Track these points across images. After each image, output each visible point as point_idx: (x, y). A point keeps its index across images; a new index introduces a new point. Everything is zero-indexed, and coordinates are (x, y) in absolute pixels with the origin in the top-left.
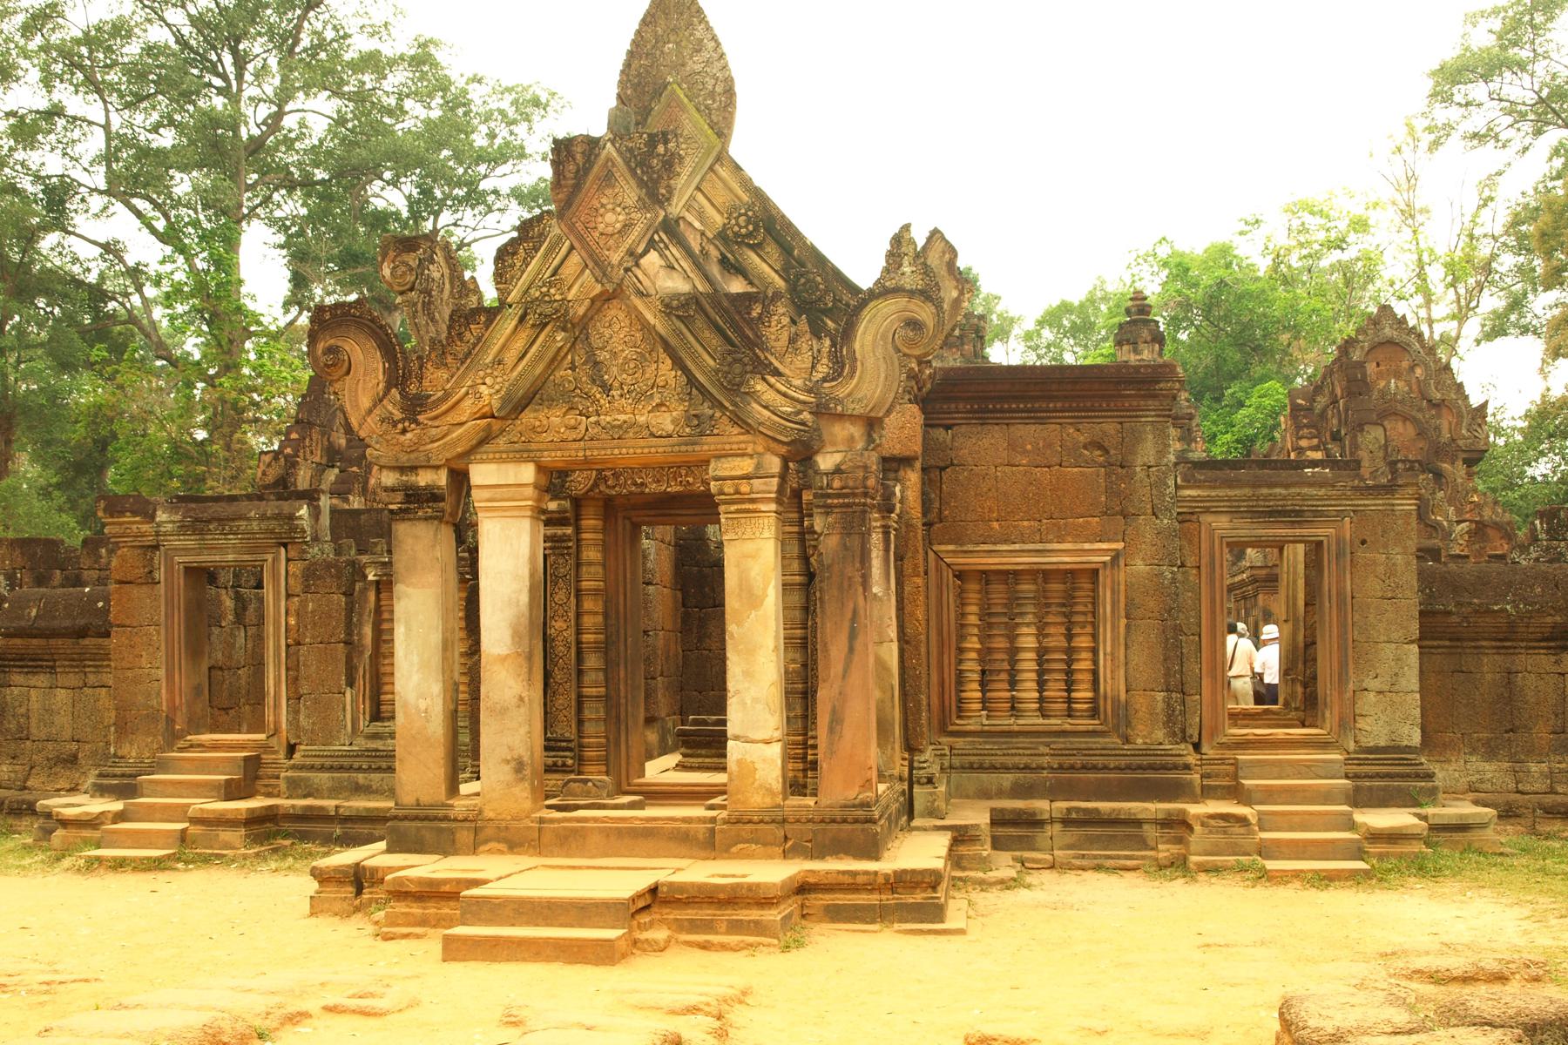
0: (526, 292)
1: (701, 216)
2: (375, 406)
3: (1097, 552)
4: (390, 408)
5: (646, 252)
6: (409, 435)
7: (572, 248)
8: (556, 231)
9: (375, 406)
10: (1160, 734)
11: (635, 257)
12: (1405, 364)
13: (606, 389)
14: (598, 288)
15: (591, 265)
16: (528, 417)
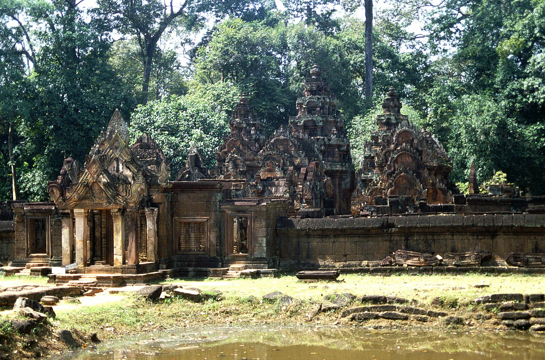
1: (122, 157)
3: (204, 219)
8: (86, 171)
10: (215, 255)
11: (98, 176)
12: (411, 138)
13: (95, 197)
16: (83, 201)
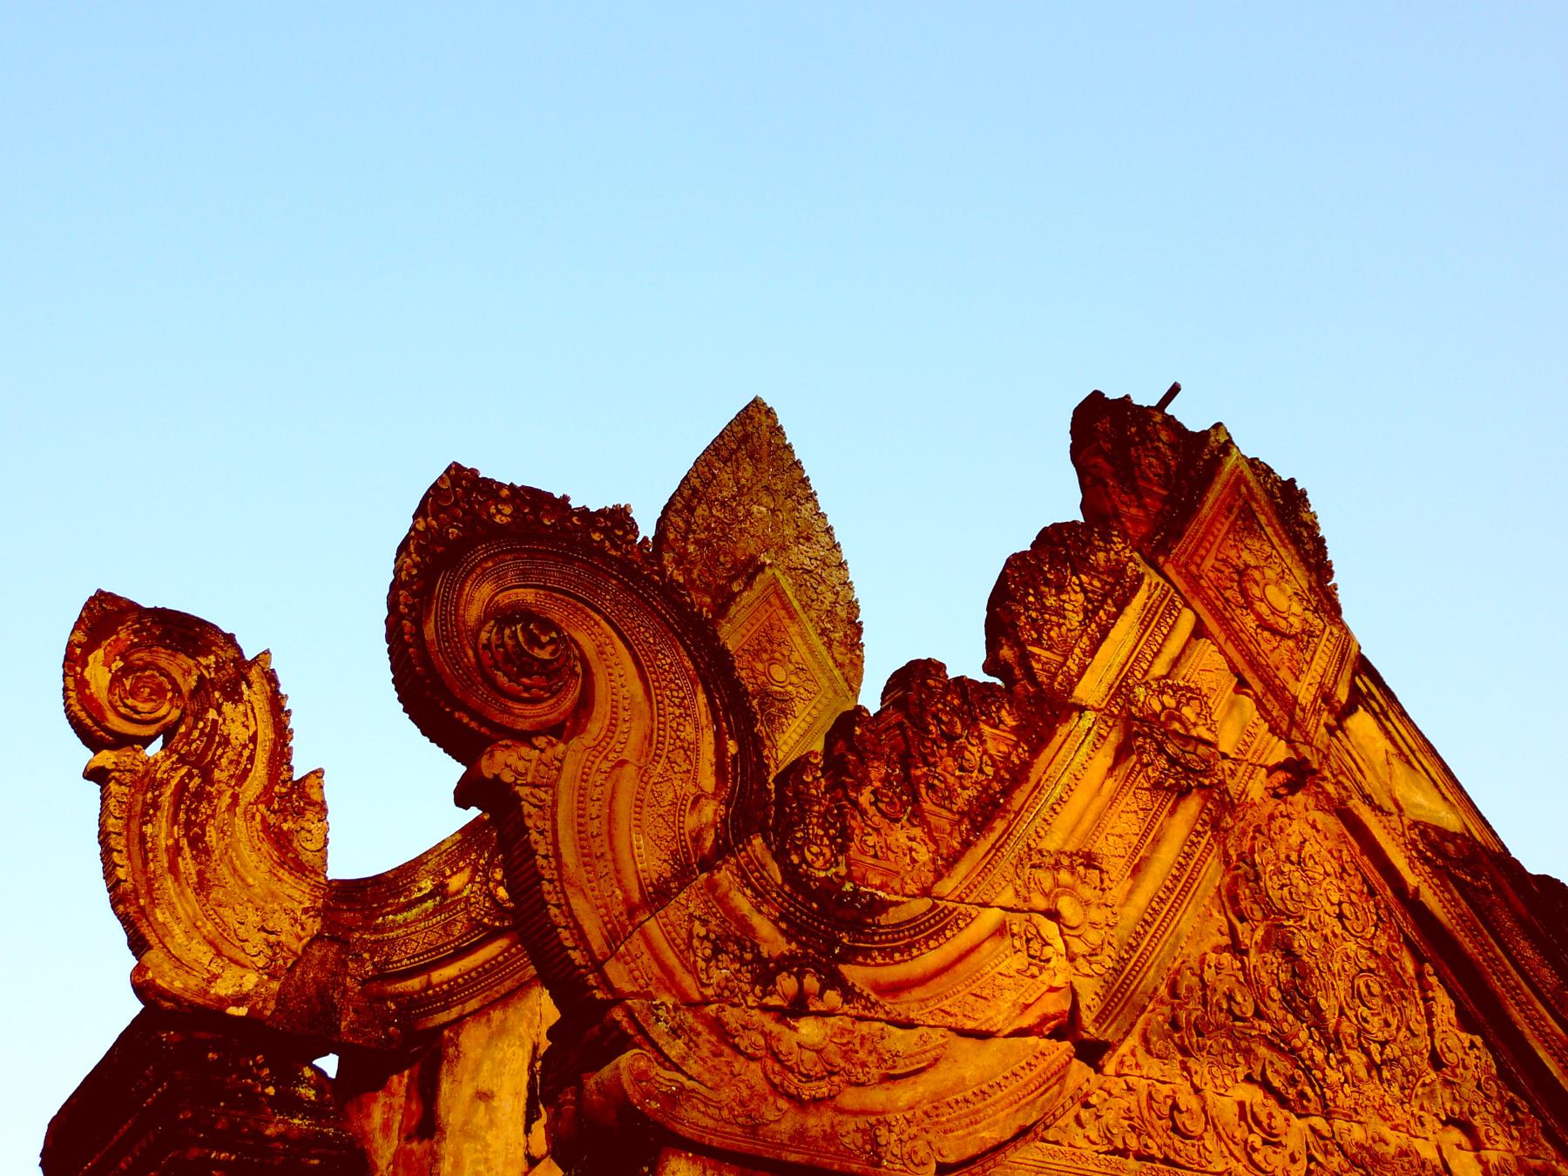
0: (1121, 690)
2: (683, 875)
4: (742, 902)
5: (1349, 710)
6: (809, 1030)
7: (1199, 631)
9: (683, 875)
14: (1279, 752)
15: (1258, 687)
